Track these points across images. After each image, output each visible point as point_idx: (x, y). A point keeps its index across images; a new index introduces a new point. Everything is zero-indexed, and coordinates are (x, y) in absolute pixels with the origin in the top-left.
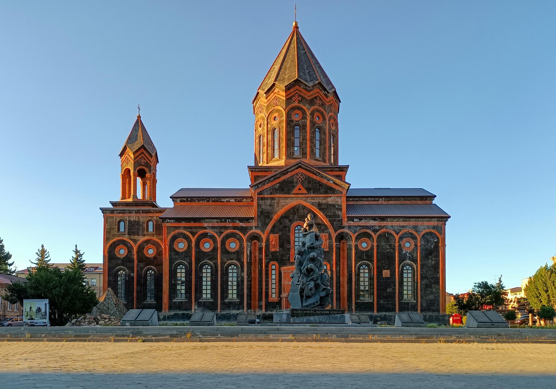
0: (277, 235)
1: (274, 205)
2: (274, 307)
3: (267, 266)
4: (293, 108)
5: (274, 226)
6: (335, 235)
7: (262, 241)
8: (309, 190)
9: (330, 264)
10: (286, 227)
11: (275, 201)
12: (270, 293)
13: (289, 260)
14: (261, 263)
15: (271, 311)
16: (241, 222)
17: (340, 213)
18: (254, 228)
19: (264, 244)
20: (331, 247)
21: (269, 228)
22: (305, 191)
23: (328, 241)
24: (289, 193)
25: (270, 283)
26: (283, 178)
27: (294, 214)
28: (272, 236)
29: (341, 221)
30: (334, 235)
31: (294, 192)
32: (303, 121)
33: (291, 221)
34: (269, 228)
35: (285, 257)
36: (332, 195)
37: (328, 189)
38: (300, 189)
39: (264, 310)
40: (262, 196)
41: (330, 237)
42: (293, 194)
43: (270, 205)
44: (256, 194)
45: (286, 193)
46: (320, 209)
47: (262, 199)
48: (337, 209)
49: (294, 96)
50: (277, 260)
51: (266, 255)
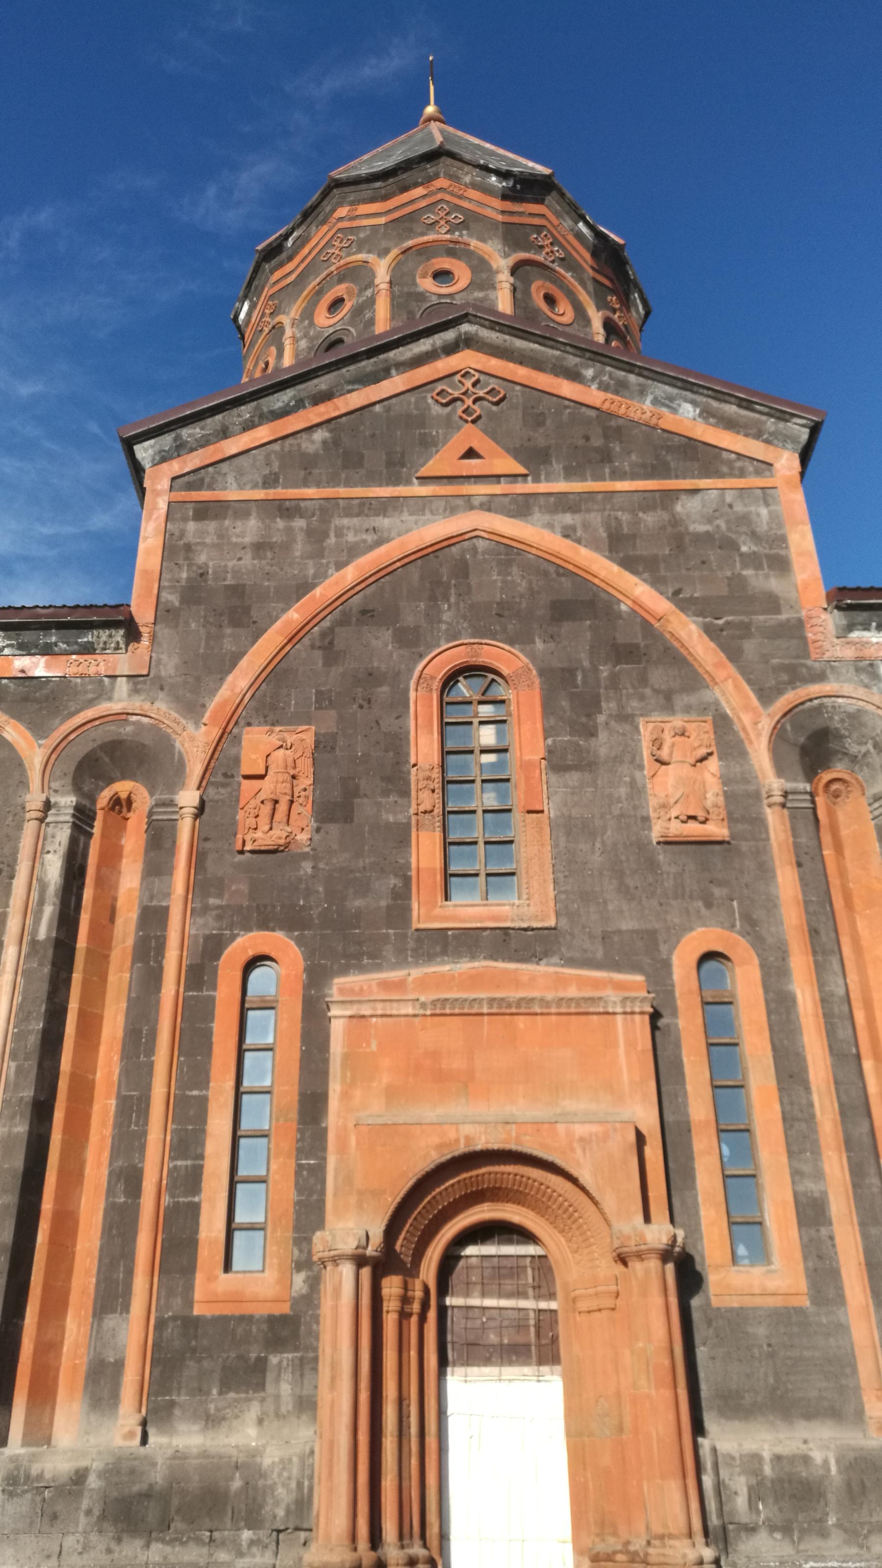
0: (305, 736)
1: (286, 547)
2: (248, 1376)
3: (199, 973)
4: (425, 252)
5: (276, 674)
6: (766, 725)
7: (176, 773)
8: (535, 459)
9: (758, 941)
10: (372, 678)
11: (299, 523)
12: (211, 1226)
13: (399, 911)
14: (149, 950)
15: (212, 1421)
16: (26, 649)
17: (774, 584)
18: (122, 685)
19: (188, 798)
20: (742, 803)
21: (239, 681)
22: (509, 465)
23: (713, 765)
24: (395, 480)
25: (219, 1125)
26: (357, 399)
27: (435, 591)
28: (257, 743)
29: (795, 630)
30: (757, 726)
31: (431, 468)
32: (479, 295)
33: (413, 641)
34: (239, 681)
35: (364, 889)
36: (703, 483)
37: (669, 449)
38: (471, 454)
39: (128, 1415)
40: (205, 495)
41: (727, 741)
42: (425, 480)
43: (259, 548)
44: (165, 484)
45: (372, 479)
46: (629, 564)
47: (204, 511)
48: (753, 561)
49: (430, 207)
50: (292, 921)
51: (202, 883)
